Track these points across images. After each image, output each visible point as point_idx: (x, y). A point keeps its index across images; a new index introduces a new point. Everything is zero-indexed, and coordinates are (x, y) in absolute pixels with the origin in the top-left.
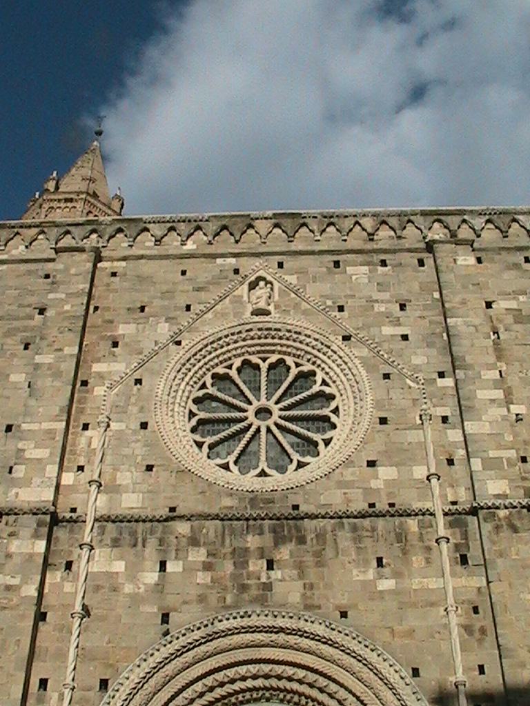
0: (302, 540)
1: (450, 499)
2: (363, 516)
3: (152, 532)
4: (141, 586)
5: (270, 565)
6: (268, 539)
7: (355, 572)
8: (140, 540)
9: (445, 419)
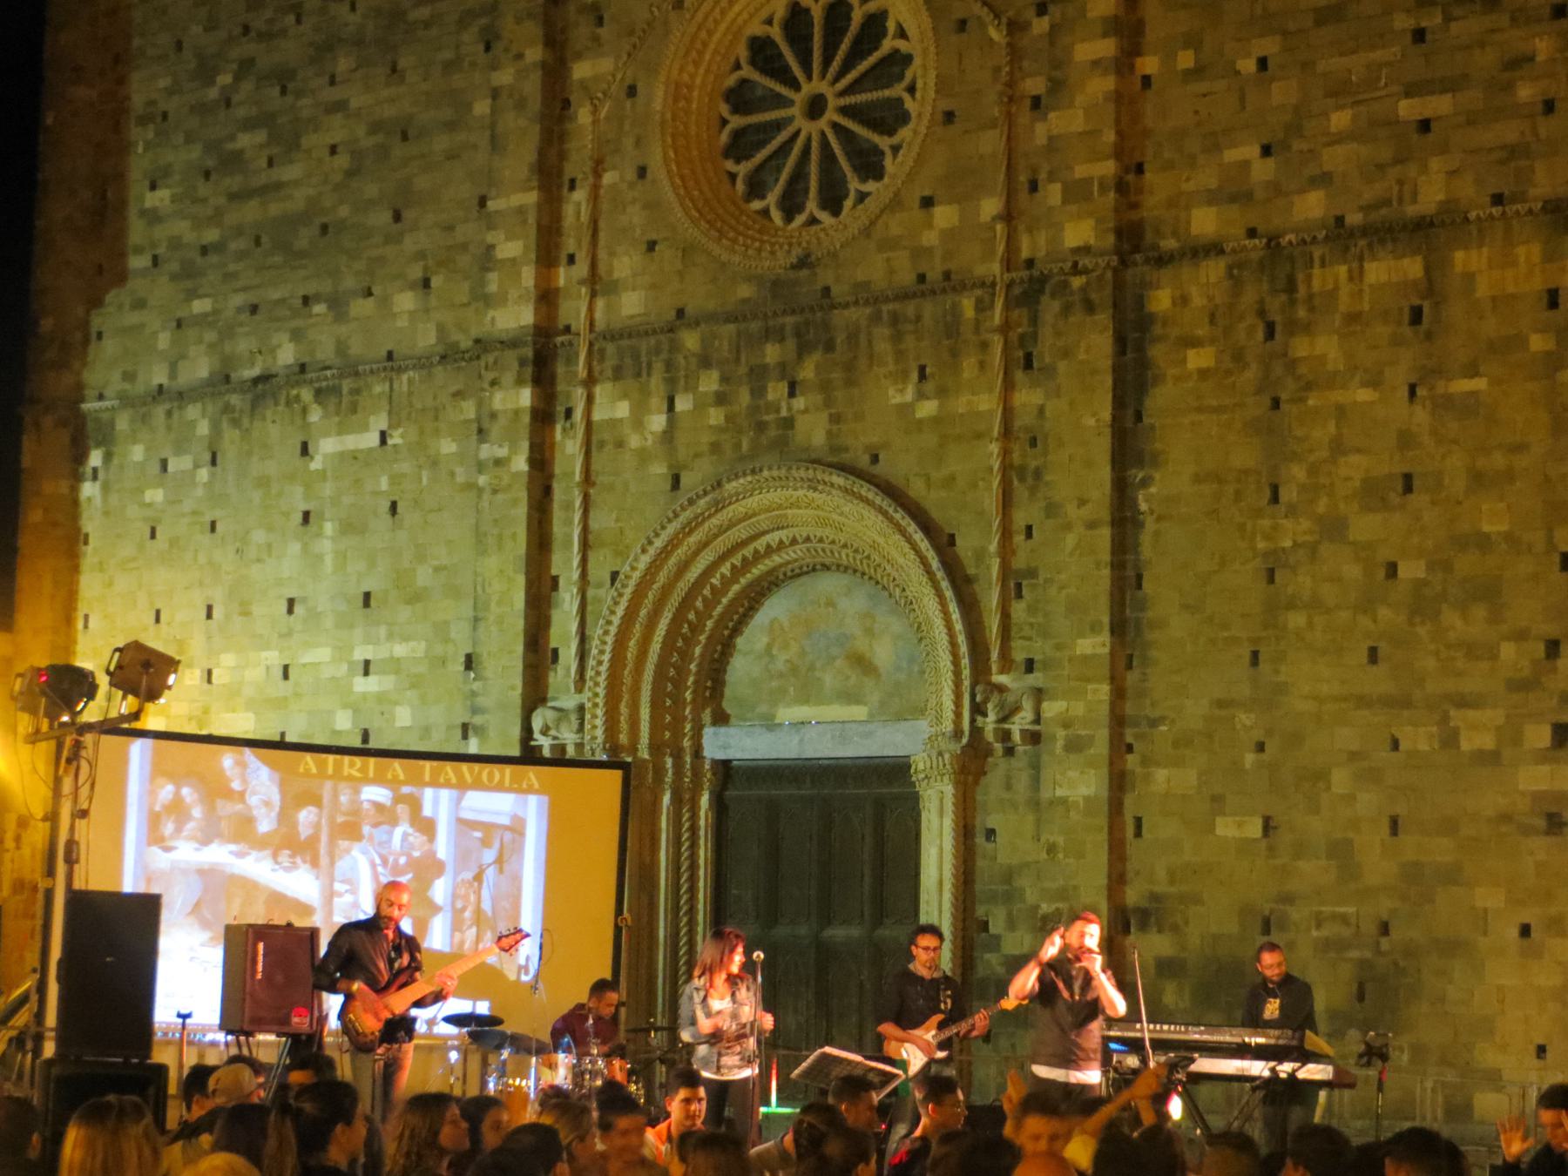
0: (829, 347)
1: (1025, 253)
2: (904, 296)
3: (657, 351)
4: (650, 437)
5: (792, 394)
6: (791, 344)
7: (891, 392)
8: (644, 365)
9: (1036, 102)
